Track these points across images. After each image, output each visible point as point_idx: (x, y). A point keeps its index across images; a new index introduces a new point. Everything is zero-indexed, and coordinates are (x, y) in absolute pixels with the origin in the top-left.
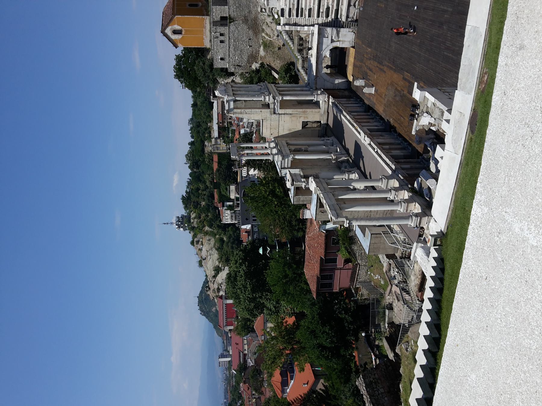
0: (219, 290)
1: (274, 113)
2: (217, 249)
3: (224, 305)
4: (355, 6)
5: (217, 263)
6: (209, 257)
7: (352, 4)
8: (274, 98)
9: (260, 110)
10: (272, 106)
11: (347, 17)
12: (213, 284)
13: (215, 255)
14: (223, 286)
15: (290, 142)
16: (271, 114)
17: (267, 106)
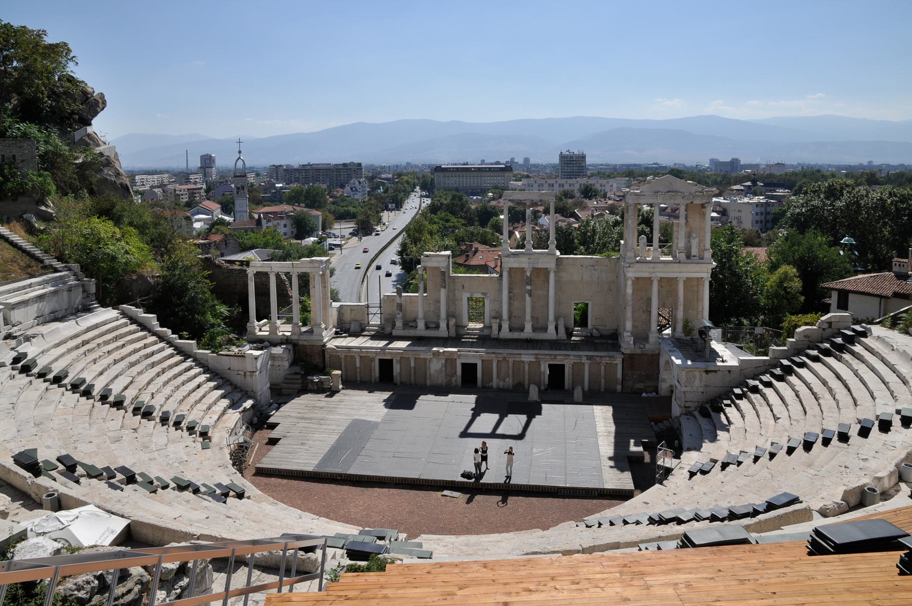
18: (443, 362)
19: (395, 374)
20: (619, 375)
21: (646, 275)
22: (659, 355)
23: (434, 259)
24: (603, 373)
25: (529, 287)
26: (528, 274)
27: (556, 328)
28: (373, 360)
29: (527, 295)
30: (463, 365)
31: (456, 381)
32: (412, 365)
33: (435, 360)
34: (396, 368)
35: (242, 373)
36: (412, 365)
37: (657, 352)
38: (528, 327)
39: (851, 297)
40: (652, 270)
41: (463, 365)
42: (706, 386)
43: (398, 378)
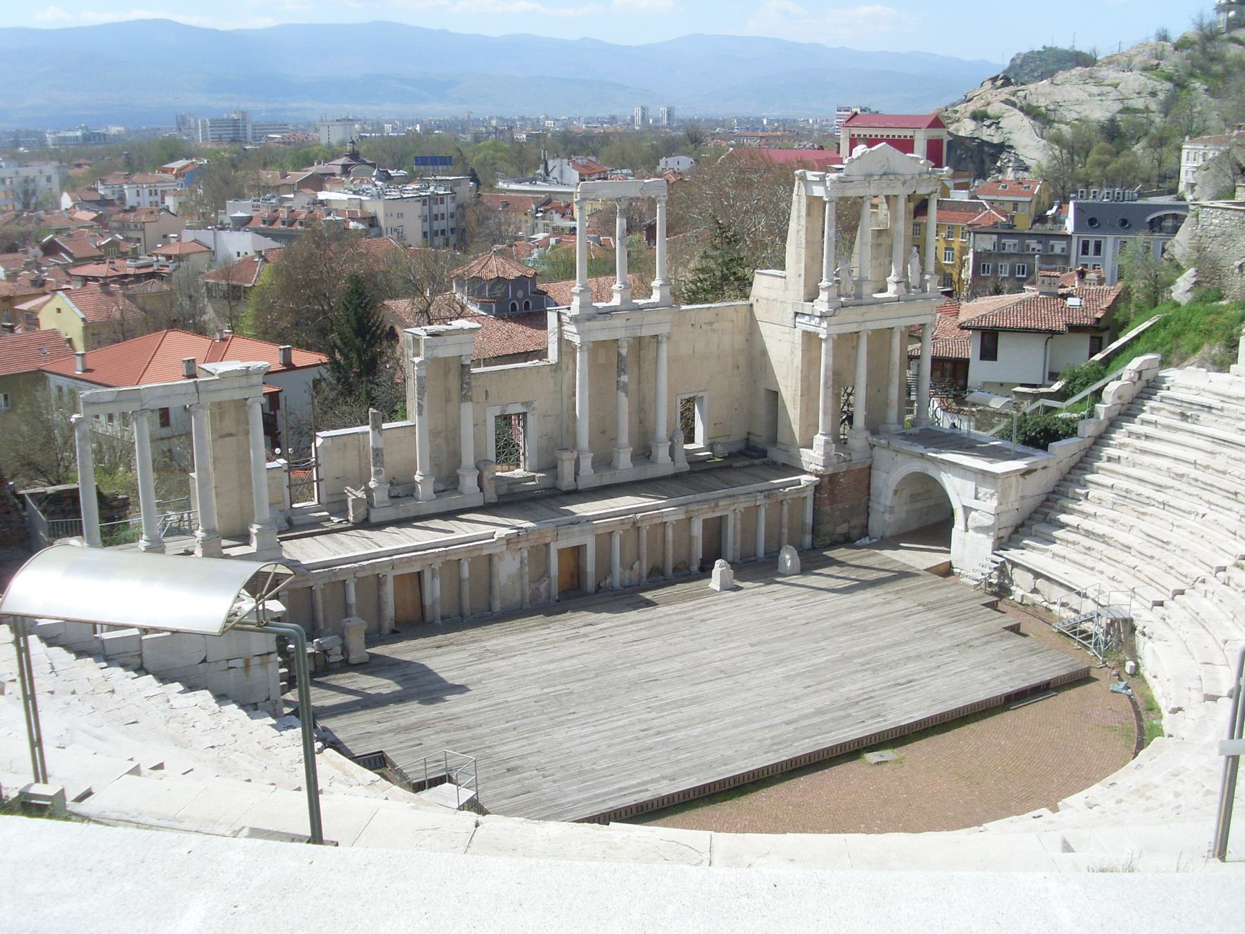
0: (978, 117)
1: (796, 314)
2: (1112, 121)
3: (909, 133)
4: (1035, 591)
5: (1071, 116)
6: (1095, 90)
7: (1040, 583)
8: (823, 316)
9: (803, 273)
10: (807, 308)
11: (1015, 565)
12: (1007, 102)
13: (1099, 113)
14: (992, 130)
15: (664, 348)
16: (793, 304)
17: (812, 297)
18: (526, 554)
19: (428, 601)
20: (809, 519)
21: (853, 328)
22: (870, 467)
23: (450, 339)
24: (785, 520)
25: (625, 378)
26: (624, 352)
27: (672, 454)
28: (379, 581)
29: (622, 395)
30: (560, 552)
31: (548, 589)
32: (466, 573)
33: (508, 557)
34: (434, 590)
35: (239, 663)
36: (466, 573)
37: (869, 462)
38: (624, 457)
39: (1002, 340)
40: (860, 319)
41: (560, 552)
42: (1023, 498)
43: (438, 611)
